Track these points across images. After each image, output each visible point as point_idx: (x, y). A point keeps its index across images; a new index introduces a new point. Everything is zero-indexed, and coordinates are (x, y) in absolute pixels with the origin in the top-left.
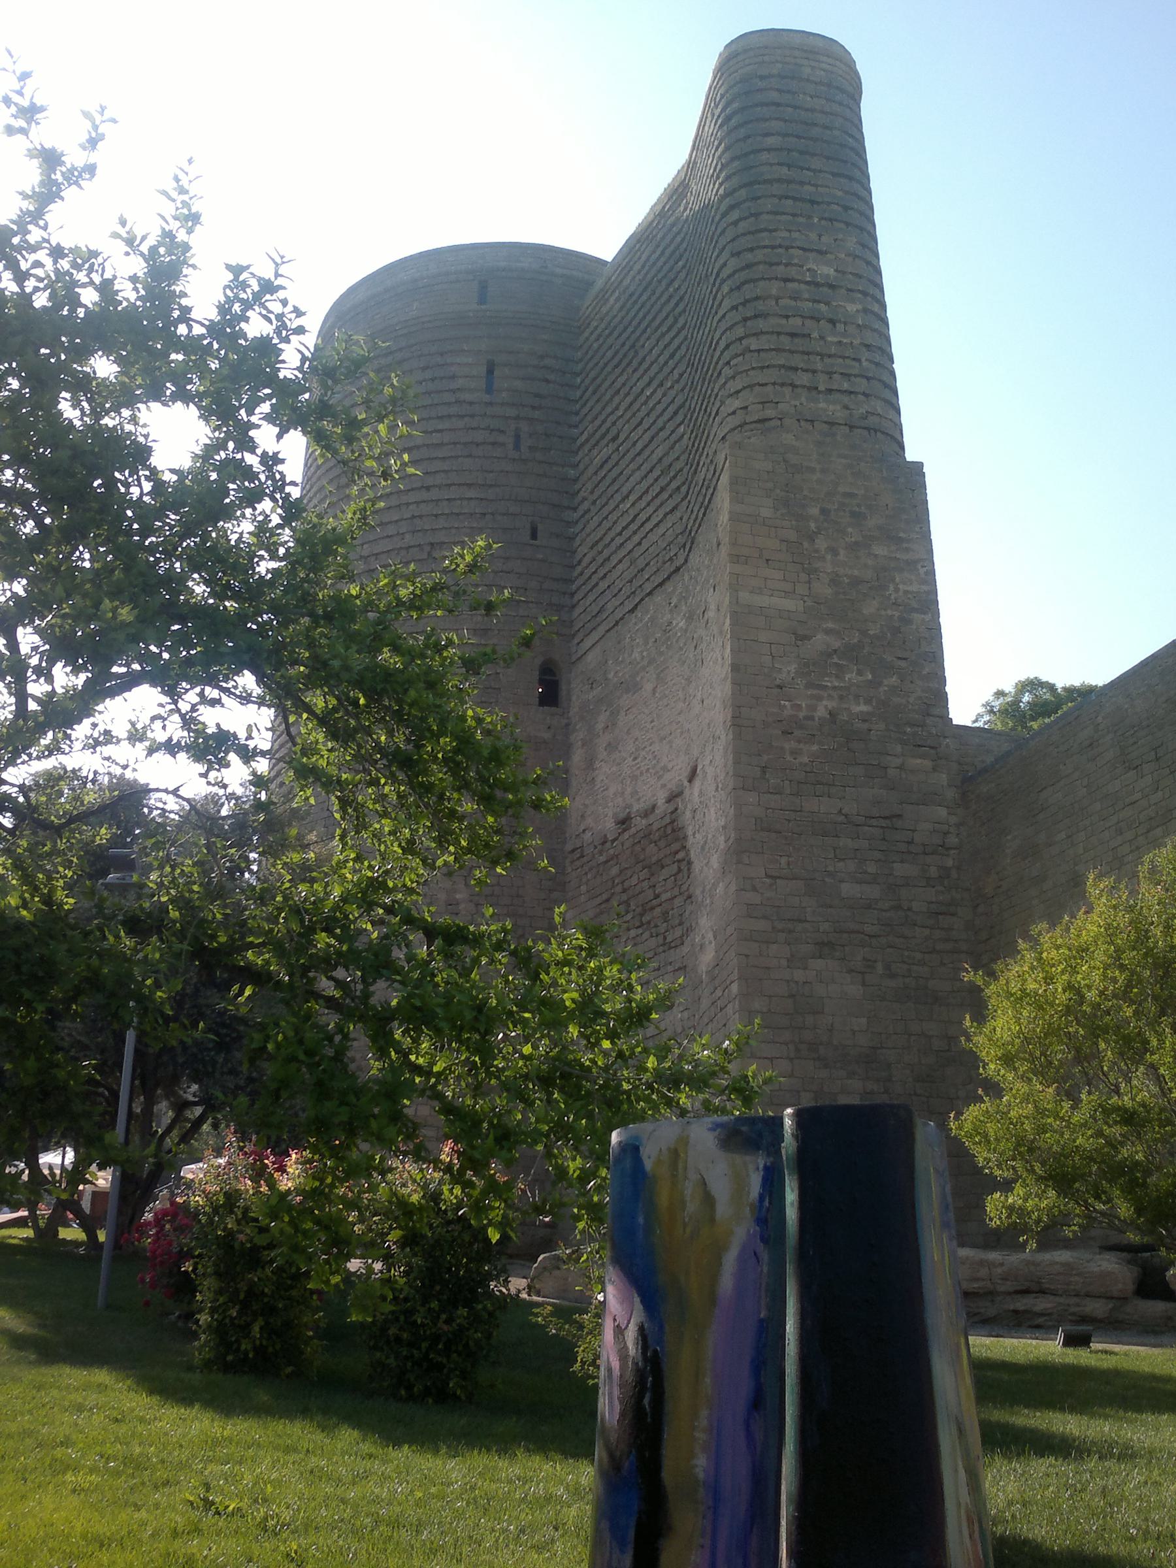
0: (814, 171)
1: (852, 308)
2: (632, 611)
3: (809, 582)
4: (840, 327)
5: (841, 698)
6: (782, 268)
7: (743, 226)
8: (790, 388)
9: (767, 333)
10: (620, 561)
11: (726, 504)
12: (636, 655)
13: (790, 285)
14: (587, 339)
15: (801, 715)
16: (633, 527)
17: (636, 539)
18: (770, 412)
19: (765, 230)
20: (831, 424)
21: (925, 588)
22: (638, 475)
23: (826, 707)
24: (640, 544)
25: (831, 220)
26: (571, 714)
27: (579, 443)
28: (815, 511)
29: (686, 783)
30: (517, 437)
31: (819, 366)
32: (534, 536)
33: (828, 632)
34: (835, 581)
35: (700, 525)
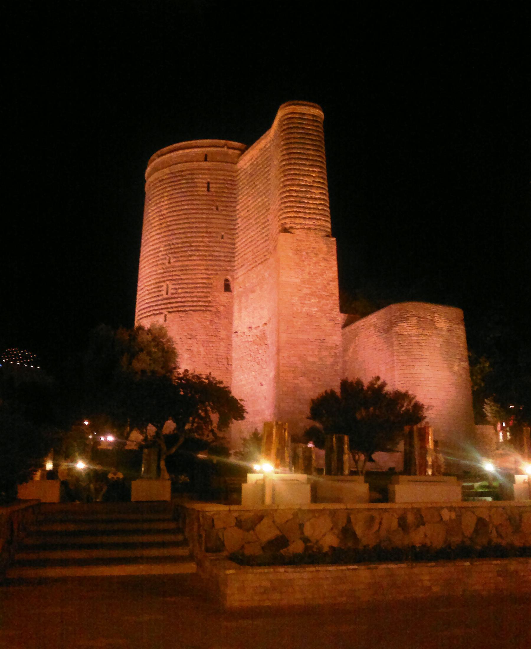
15: (299, 311)
23: (305, 309)
28: (304, 253)
33: (307, 288)
34: (309, 274)
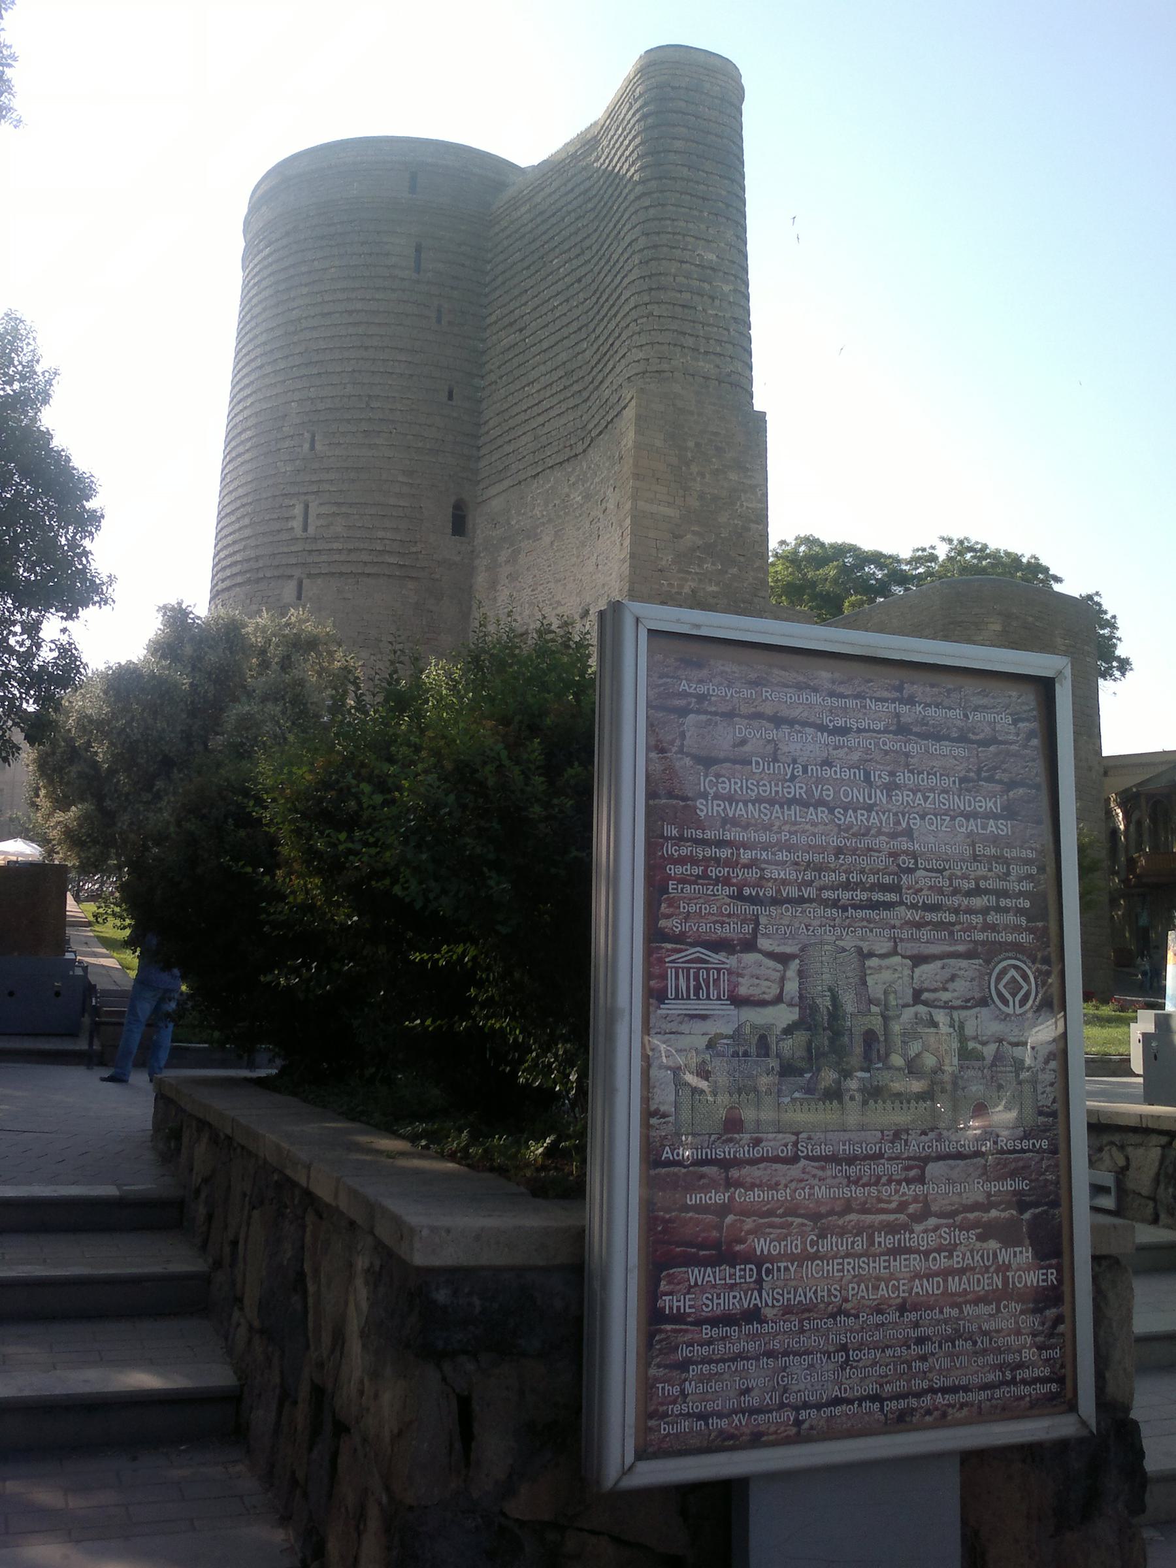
0: (707, 173)
1: (727, 288)
2: (534, 477)
3: (684, 497)
4: (717, 302)
5: (700, 580)
6: (680, 250)
7: (652, 212)
8: (680, 348)
9: (666, 303)
10: (524, 434)
11: (631, 434)
12: (537, 512)
13: (684, 266)
14: (497, 234)
16: (536, 410)
17: (541, 420)
18: (665, 366)
19: (670, 219)
20: (706, 378)
21: (760, 505)
22: (543, 369)
24: (543, 425)
25: (716, 215)
26: (475, 543)
27: (489, 320)
28: (691, 444)
29: (577, 617)
30: (439, 311)
31: (701, 333)
32: (450, 397)
33: (694, 533)
34: (701, 497)
35: (601, 433)
